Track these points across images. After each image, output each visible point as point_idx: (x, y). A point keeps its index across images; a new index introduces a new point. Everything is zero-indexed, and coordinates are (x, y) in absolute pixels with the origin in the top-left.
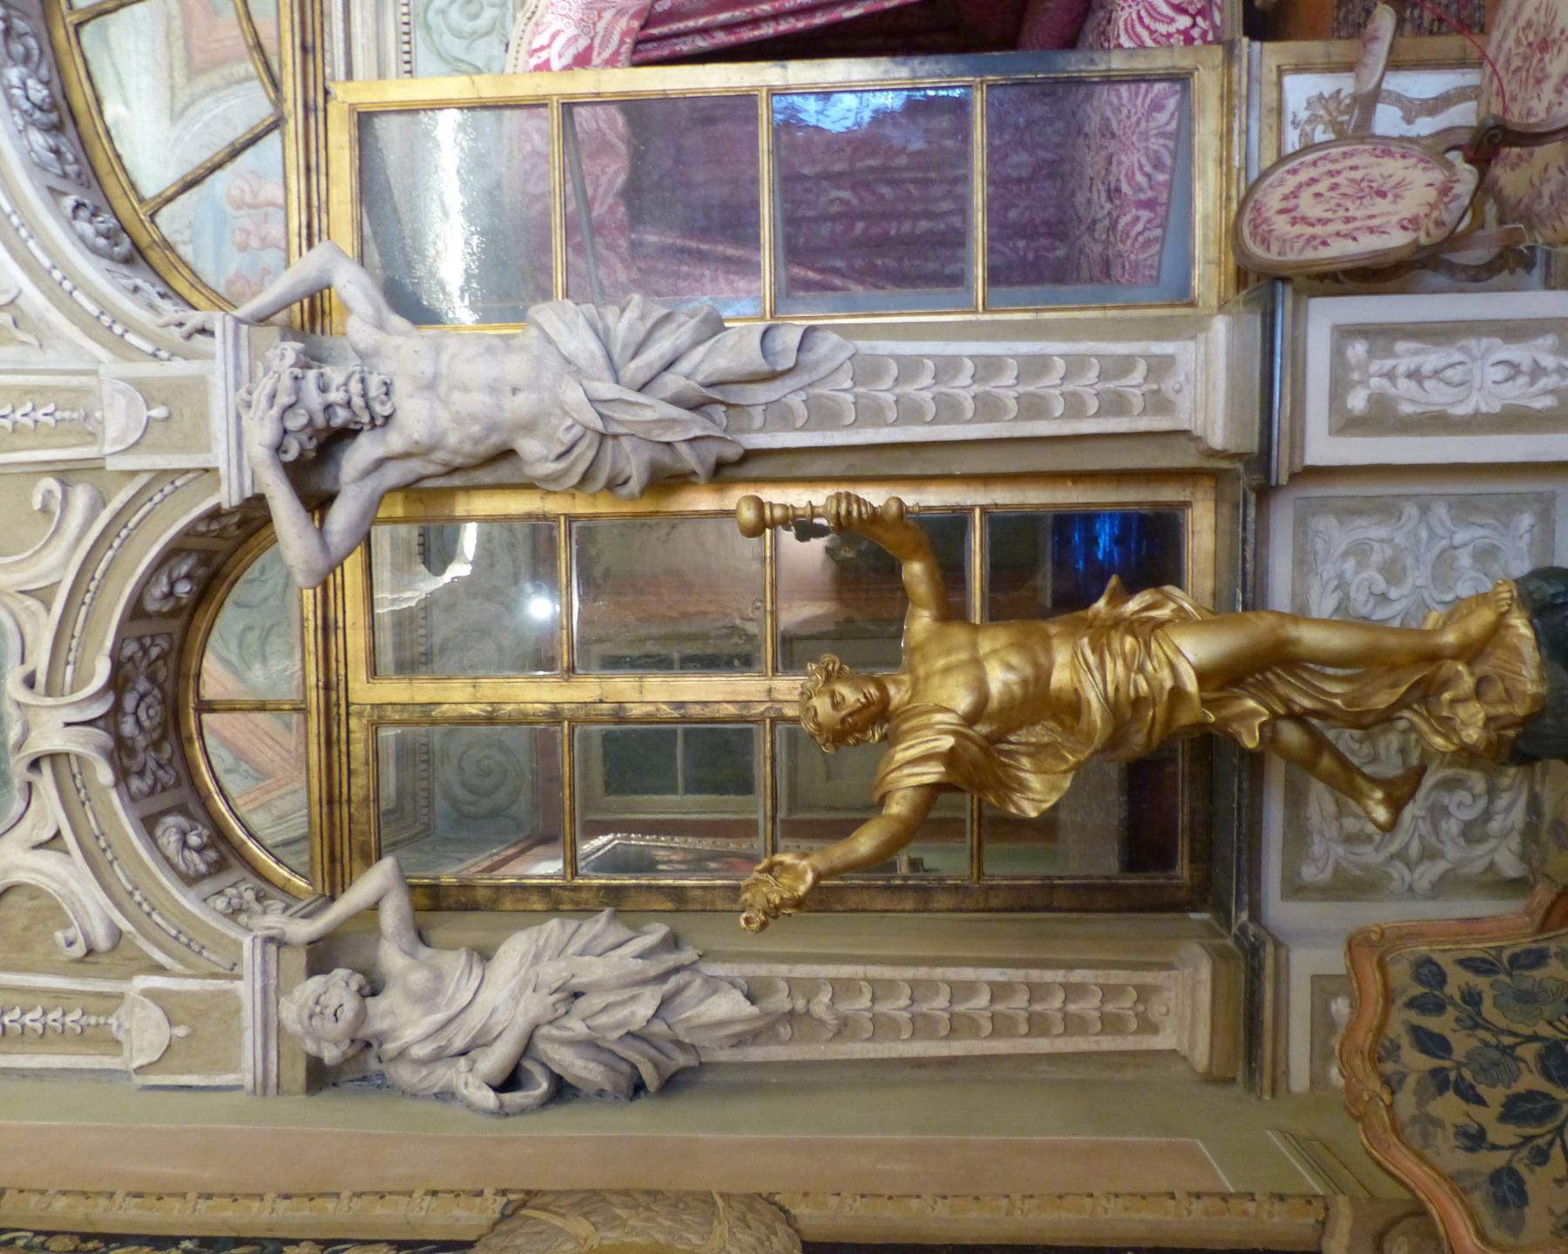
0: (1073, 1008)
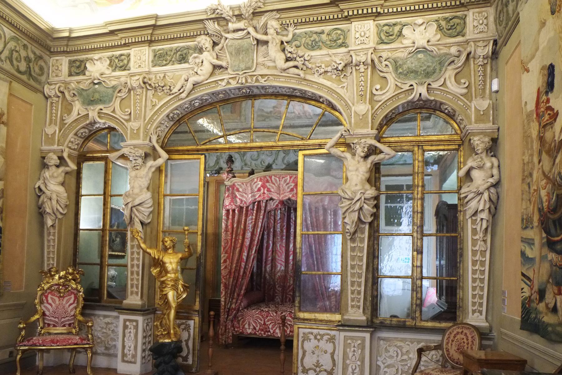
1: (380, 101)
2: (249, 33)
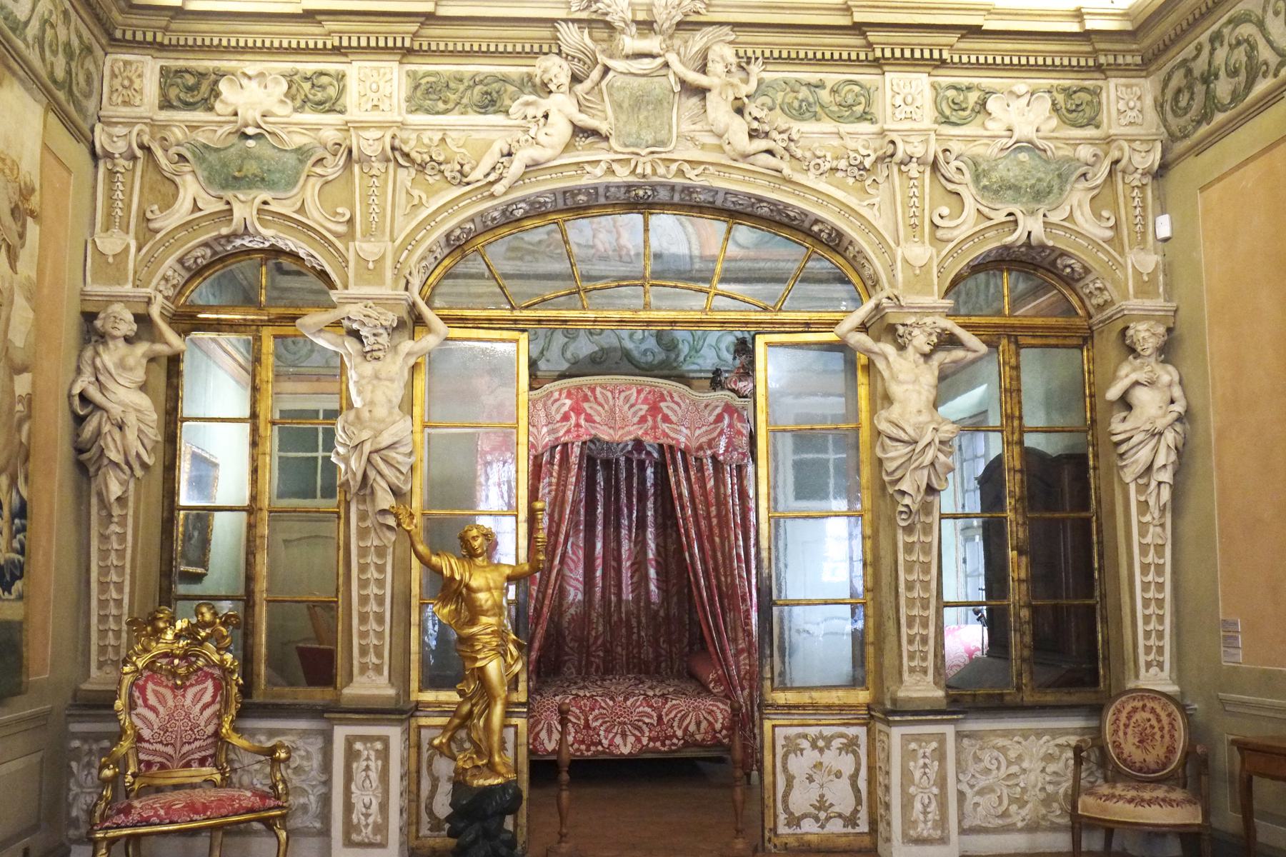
0: (110, 634)
2: (666, 65)
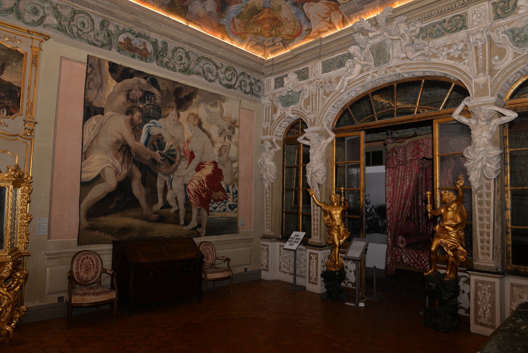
1: (499, 70)
